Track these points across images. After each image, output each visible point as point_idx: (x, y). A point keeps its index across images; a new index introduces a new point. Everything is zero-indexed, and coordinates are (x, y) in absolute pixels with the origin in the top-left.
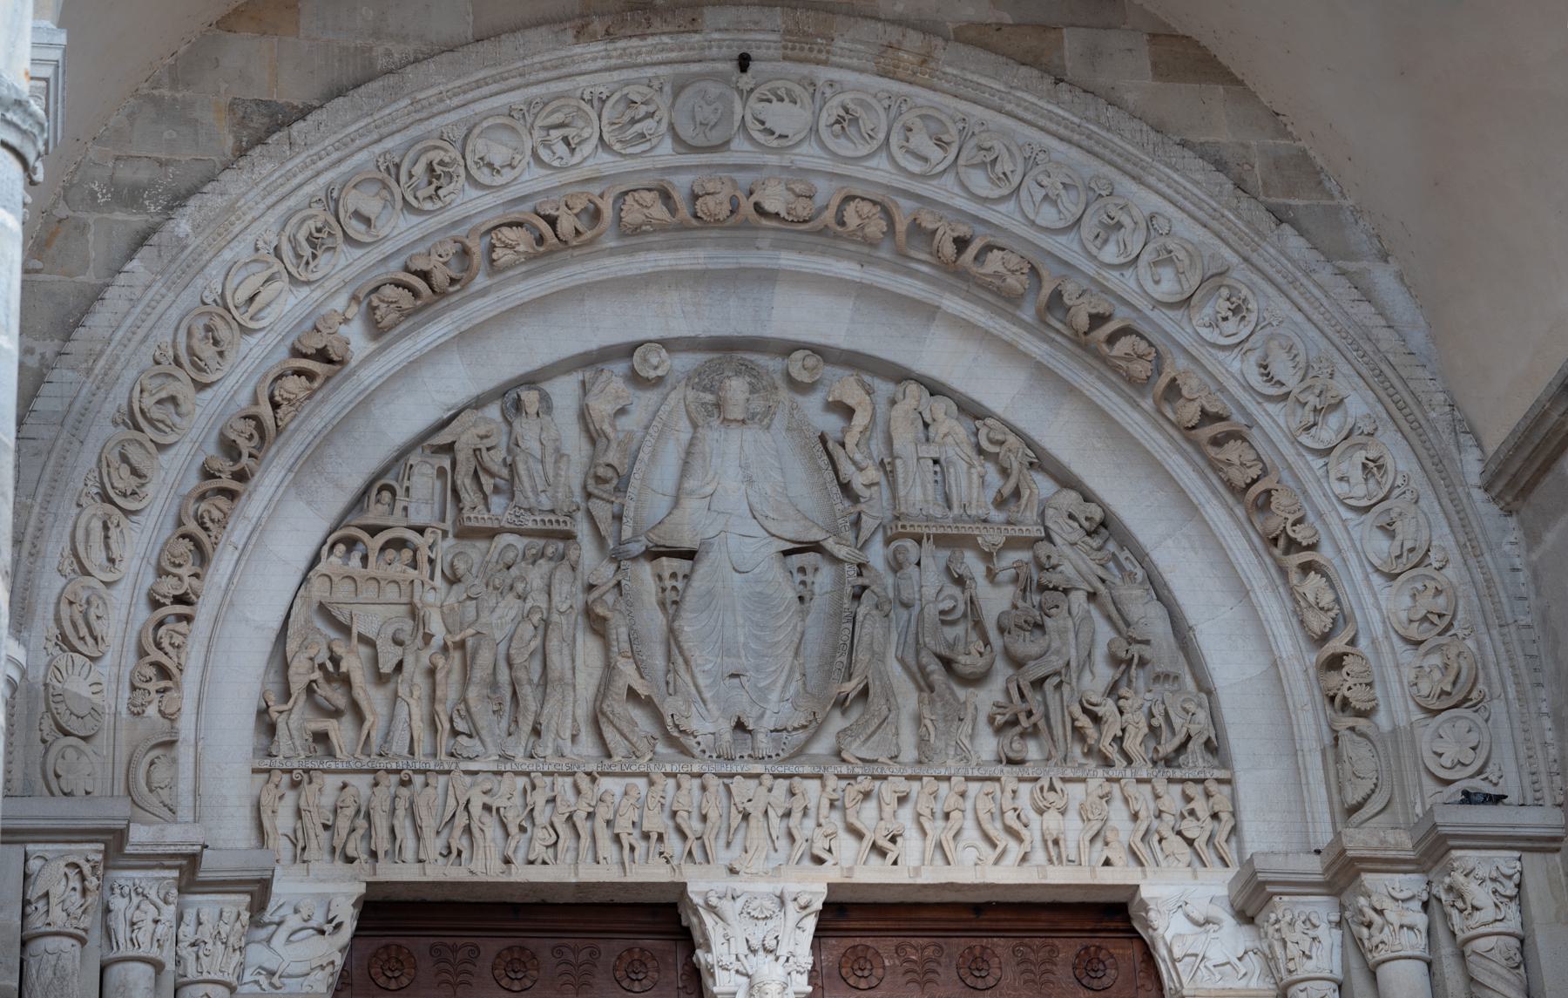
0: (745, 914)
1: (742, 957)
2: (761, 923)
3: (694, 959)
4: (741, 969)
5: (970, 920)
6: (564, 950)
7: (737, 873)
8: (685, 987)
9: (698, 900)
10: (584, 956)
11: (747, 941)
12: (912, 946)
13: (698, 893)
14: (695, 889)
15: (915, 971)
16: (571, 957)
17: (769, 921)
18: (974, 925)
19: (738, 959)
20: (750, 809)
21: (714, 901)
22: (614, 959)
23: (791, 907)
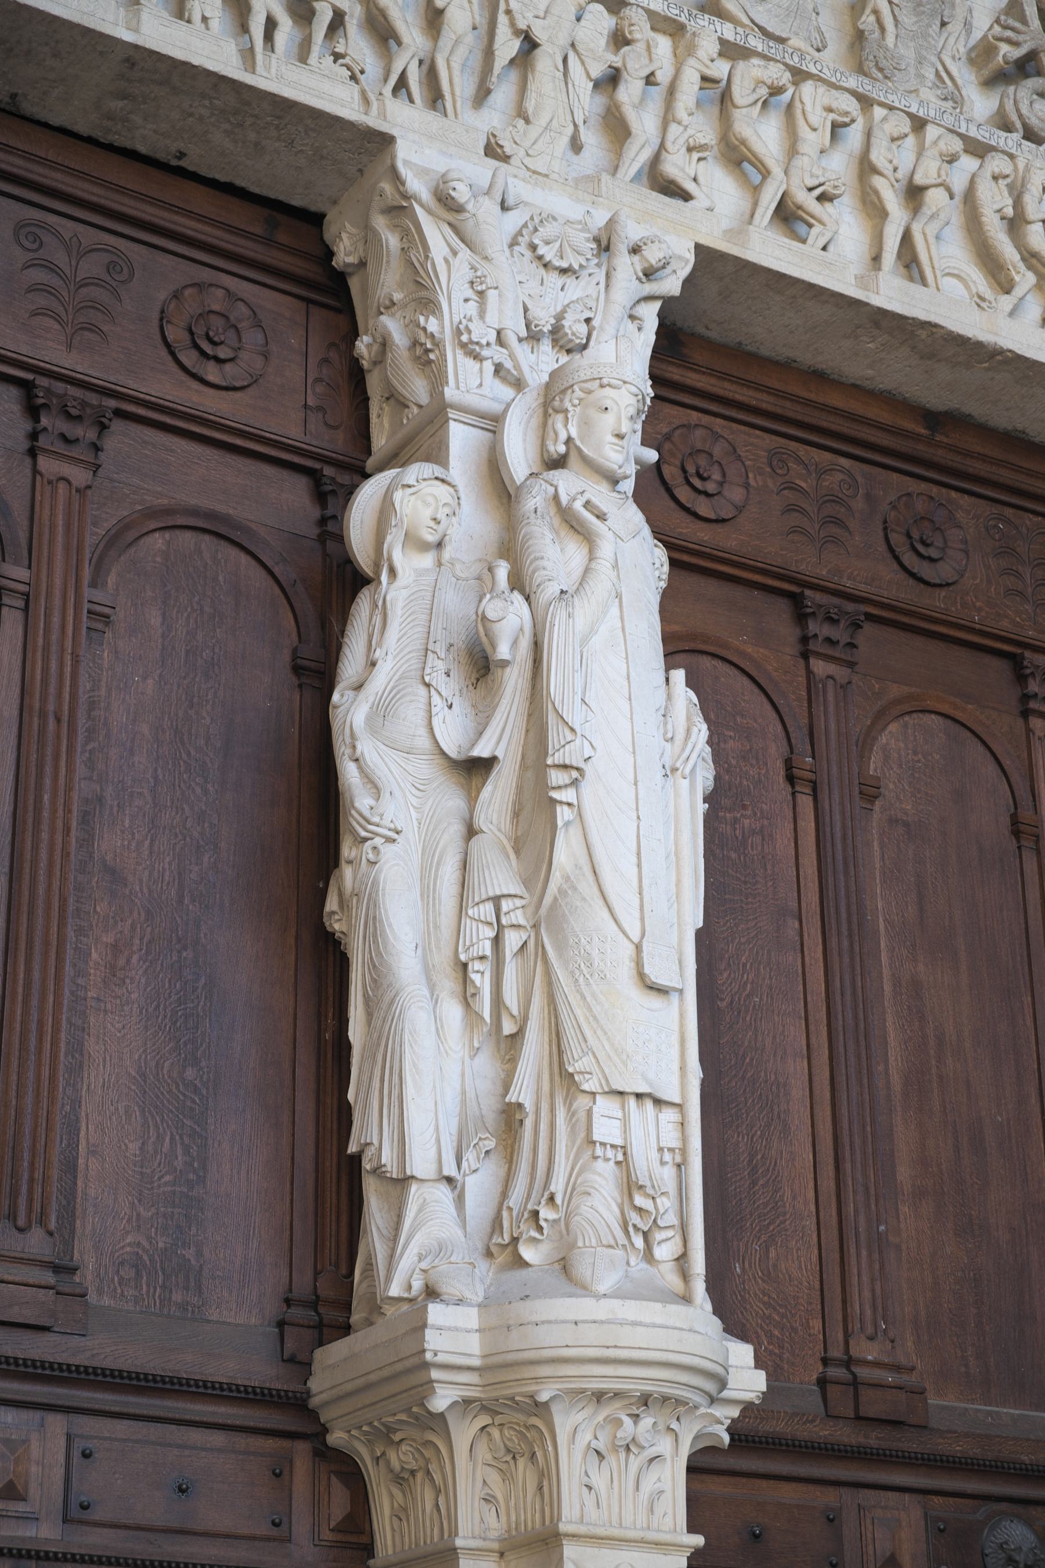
0: (522, 248)
1: (512, 339)
2: (554, 279)
3: (363, 346)
4: (508, 364)
5: (916, 437)
6: (47, 238)
7: (505, 159)
8: (319, 409)
9: (415, 184)
10: (91, 267)
11: (526, 310)
12: (799, 461)
13: (422, 172)
14: (415, 159)
15: (802, 511)
16: (61, 258)
17: (569, 281)
18: (921, 450)
19: (500, 340)
20: (539, 33)
21: (461, 193)
22: (162, 295)
23: (626, 267)
